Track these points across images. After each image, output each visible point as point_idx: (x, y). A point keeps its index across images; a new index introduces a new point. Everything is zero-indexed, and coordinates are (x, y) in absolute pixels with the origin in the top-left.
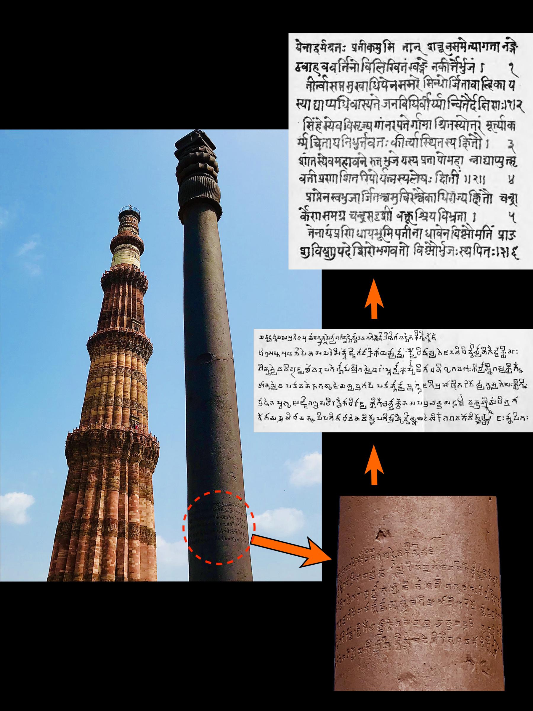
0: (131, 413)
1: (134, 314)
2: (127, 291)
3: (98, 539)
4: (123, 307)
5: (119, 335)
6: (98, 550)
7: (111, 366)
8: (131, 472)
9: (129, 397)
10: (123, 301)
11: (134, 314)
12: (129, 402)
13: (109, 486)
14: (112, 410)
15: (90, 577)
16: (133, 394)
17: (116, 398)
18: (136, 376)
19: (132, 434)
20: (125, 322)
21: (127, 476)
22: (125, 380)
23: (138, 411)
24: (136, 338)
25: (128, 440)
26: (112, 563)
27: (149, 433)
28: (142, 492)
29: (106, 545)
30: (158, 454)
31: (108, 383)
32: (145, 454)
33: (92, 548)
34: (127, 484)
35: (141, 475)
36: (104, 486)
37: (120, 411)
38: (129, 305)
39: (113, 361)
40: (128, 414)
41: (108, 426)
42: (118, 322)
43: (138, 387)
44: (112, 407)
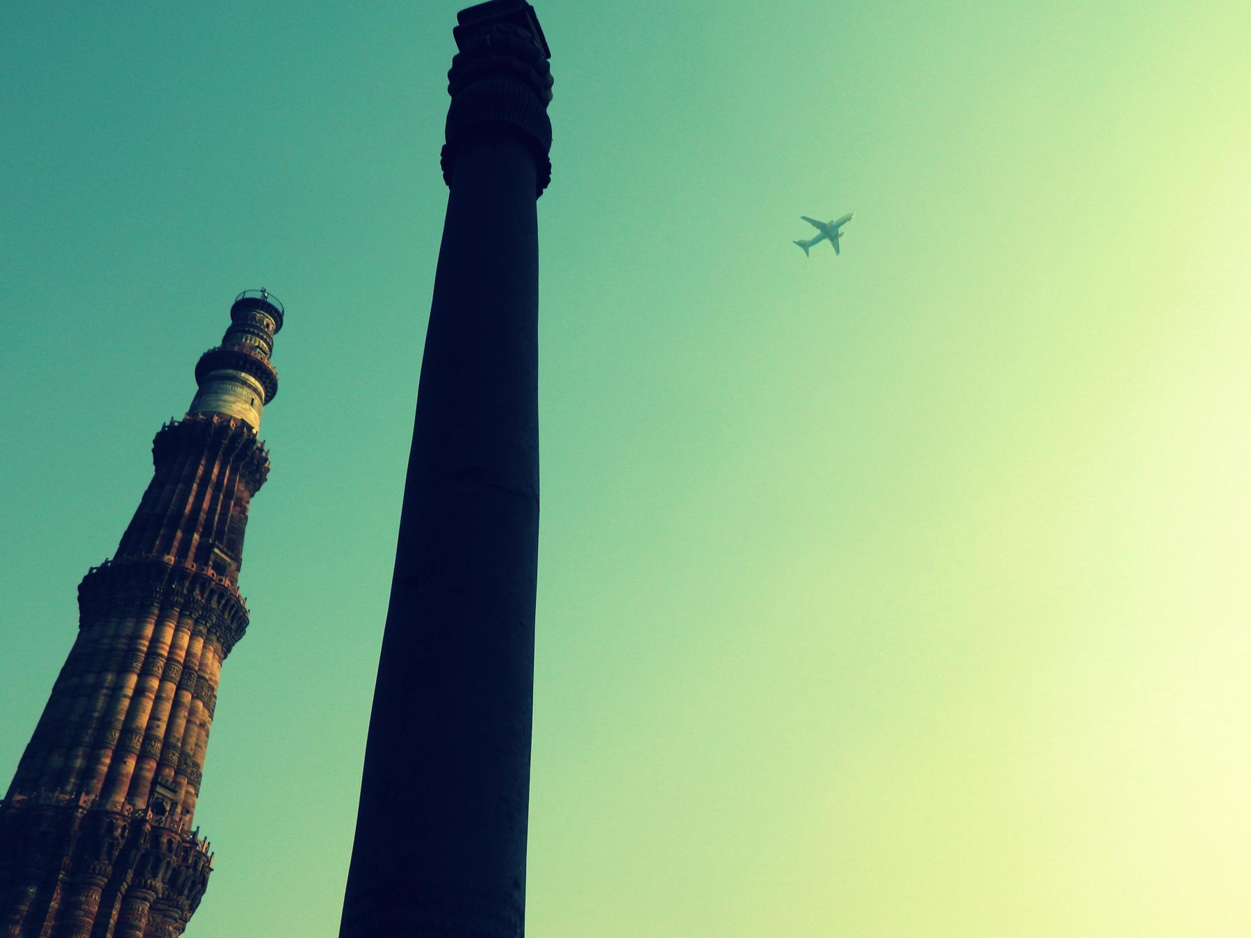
0: (158, 772)
2: (214, 477)
7: (132, 651)
11: (220, 533)
12: (159, 745)
14: (108, 761)
18: (193, 683)
20: (193, 549)
25: (132, 842)
27: (194, 829)
32: (172, 883)
37: (131, 765)
38: (212, 510)
39: (141, 637)
40: (150, 775)
42: (176, 544)
43: (192, 712)
44: (110, 753)
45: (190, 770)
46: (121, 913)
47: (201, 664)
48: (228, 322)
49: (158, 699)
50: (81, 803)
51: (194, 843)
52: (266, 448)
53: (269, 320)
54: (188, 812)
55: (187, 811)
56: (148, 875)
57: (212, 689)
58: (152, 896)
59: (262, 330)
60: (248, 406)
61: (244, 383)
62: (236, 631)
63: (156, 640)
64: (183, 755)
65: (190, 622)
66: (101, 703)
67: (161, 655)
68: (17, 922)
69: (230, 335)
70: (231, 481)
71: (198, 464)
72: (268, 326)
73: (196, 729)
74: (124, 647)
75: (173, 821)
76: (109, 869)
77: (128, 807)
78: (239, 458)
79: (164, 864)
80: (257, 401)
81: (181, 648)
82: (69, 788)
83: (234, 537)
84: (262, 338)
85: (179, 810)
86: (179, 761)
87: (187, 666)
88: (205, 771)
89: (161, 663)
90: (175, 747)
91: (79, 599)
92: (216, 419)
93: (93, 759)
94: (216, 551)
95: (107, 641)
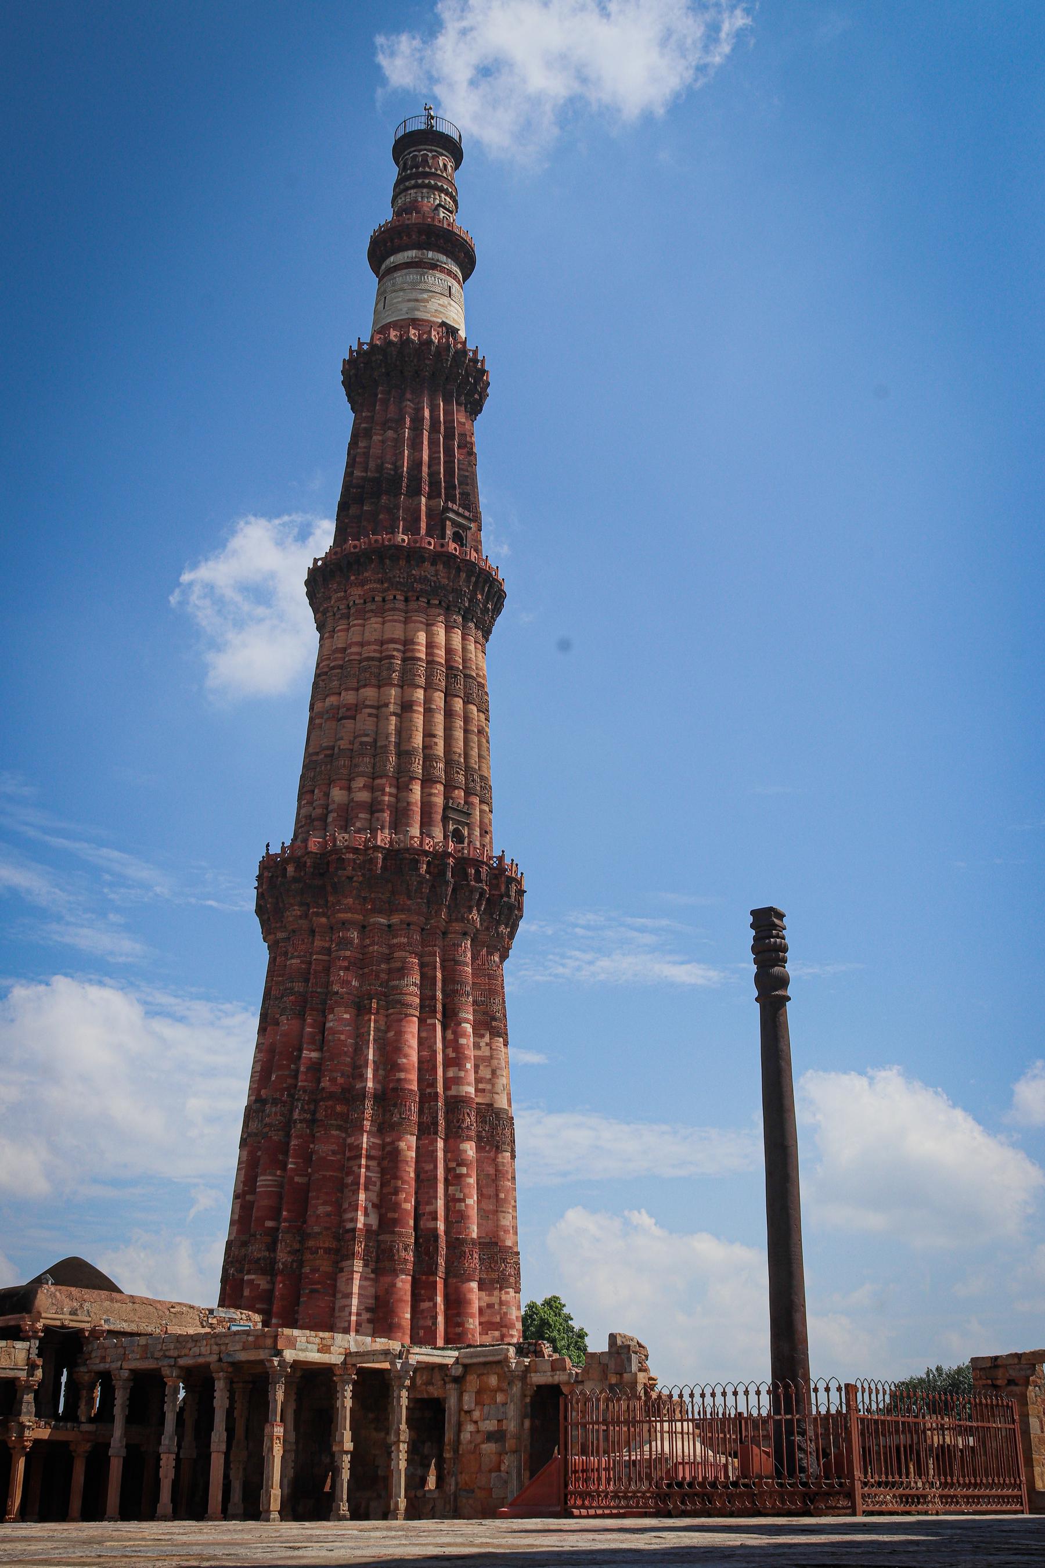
0: (446, 798)
9: (440, 750)
10: (416, 445)
11: (450, 487)
12: (441, 765)
13: (393, 1005)
14: (394, 791)
15: (348, 1236)
16: (454, 743)
19: (451, 861)
21: (439, 975)
22: (428, 700)
27: (496, 853)
28: (480, 1017)
30: (520, 909)
31: (378, 708)
33: (352, 1163)
34: (439, 995)
38: (433, 460)
40: (439, 800)
41: (383, 838)
43: (467, 720)
44: (394, 782)
45: (478, 788)
47: (465, 661)
48: (393, 172)
49: (428, 711)
50: (379, 843)
52: (480, 358)
55: (484, 832)
56: (463, 910)
57: (481, 686)
60: (445, 300)
62: (493, 610)
65: (441, 611)
67: (419, 659)
68: (347, 969)
69: (401, 187)
70: (448, 413)
72: (445, 166)
74: (377, 655)
75: (475, 848)
77: (427, 840)
81: (439, 648)
82: (358, 825)
84: (441, 190)
85: (477, 833)
86: (466, 779)
87: (450, 667)
88: (495, 781)
89: (422, 668)
90: (459, 763)
91: (310, 595)
94: (451, 515)
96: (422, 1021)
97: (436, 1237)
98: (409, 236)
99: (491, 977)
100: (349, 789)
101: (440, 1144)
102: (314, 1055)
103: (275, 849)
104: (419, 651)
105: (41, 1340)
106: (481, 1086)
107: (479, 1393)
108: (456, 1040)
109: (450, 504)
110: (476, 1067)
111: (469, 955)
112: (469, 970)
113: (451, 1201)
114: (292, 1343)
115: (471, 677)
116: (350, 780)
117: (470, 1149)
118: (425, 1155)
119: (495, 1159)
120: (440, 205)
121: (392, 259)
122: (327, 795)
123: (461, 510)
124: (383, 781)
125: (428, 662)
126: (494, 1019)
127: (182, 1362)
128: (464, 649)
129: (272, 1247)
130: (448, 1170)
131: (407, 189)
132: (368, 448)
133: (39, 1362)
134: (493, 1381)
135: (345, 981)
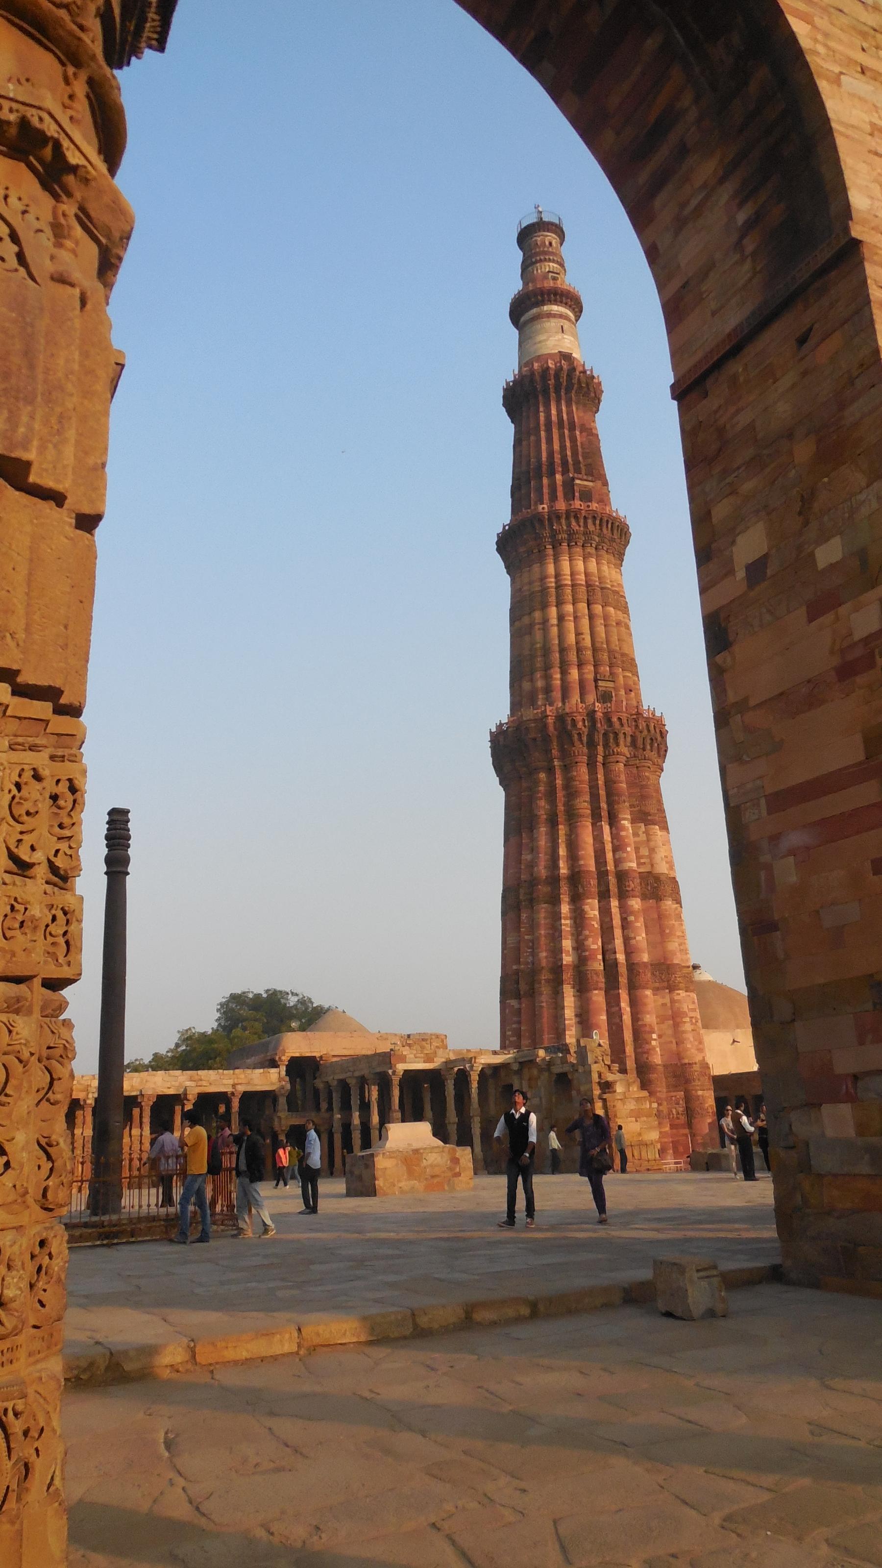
0: (596, 673)
1: (577, 463)
2: (554, 418)
3: (565, 909)
4: (551, 454)
5: (550, 519)
6: (566, 924)
7: (544, 590)
8: (610, 783)
9: (587, 641)
11: (577, 463)
13: (572, 817)
14: (558, 676)
17: (563, 650)
21: (602, 792)
22: (575, 612)
23: (613, 661)
24: (585, 518)
26: (595, 944)
29: (579, 918)
32: (634, 743)
33: (558, 923)
35: (631, 785)
36: (561, 818)
37: (574, 673)
38: (563, 447)
39: (546, 577)
40: (590, 676)
42: (546, 490)
43: (606, 617)
44: (558, 670)
46: (606, 775)
50: (548, 713)
51: (639, 714)
53: (551, 237)
54: (631, 691)
55: (631, 689)
57: (617, 592)
58: (623, 759)
59: (545, 253)
60: (560, 336)
61: (550, 315)
63: (558, 575)
64: (611, 652)
66: (538, 635)
67: (566, 585)
70: (570, 413)
71: (538, 412)
72: (550, 244)
73: (615, 630)
76: (585, 750)
78: (568, 390)
79: (621, 736)
80: (566, 325)
81: (579, 574)
82: (540, 703)
83: (590, 461)
84: (550, 260)
85: (622, 692)
87: (588, 585)
89: (568, 591)
92: (536, 365)
93: (548, 677)
95: (526, 588)
96: (593, 824)
97: (616, 963)
98: (529, 299)
99: (643, 787)
100: (532, 680)
101: (614, 903)
102: (529, 857)
103: (494, 730)
104: (565, 579)
105: (287, 1066)
106: (642, 861)
107: (530, 1079)
108: (618, 834)
109: (576, 475)
110: (637, 849)
111: (623, 777)
112: (624, 785)
113: (626, 940)
114: (403, 1059)
115: (608, 589)
116: (532, 674)
117: (635, 903)
118: (605, 911)
119: (658, 907)
120: (549, 272)
121: (523, 319)
122: (521, 687)
123: (585, 477)
124: (552, 671)
125: (573, 586)
126: (649, 814)
127: (357, 1074)
128: (599, 570)
129: (518, 983)
130: (624, 920)
131: (527, 267)
132: (521, 451)
133: (287, 1078)
134: (535, 1072)
135: (542, 806)
